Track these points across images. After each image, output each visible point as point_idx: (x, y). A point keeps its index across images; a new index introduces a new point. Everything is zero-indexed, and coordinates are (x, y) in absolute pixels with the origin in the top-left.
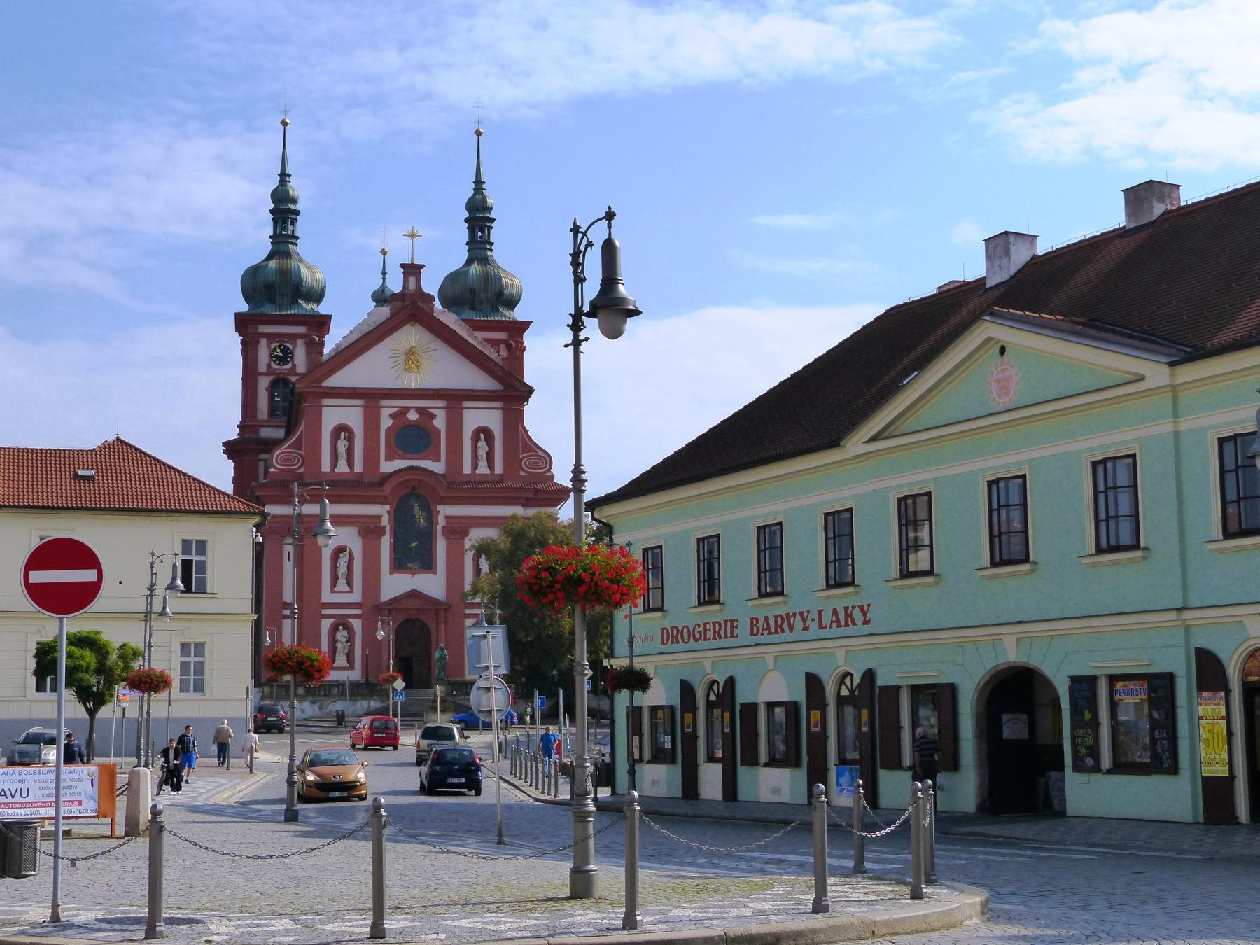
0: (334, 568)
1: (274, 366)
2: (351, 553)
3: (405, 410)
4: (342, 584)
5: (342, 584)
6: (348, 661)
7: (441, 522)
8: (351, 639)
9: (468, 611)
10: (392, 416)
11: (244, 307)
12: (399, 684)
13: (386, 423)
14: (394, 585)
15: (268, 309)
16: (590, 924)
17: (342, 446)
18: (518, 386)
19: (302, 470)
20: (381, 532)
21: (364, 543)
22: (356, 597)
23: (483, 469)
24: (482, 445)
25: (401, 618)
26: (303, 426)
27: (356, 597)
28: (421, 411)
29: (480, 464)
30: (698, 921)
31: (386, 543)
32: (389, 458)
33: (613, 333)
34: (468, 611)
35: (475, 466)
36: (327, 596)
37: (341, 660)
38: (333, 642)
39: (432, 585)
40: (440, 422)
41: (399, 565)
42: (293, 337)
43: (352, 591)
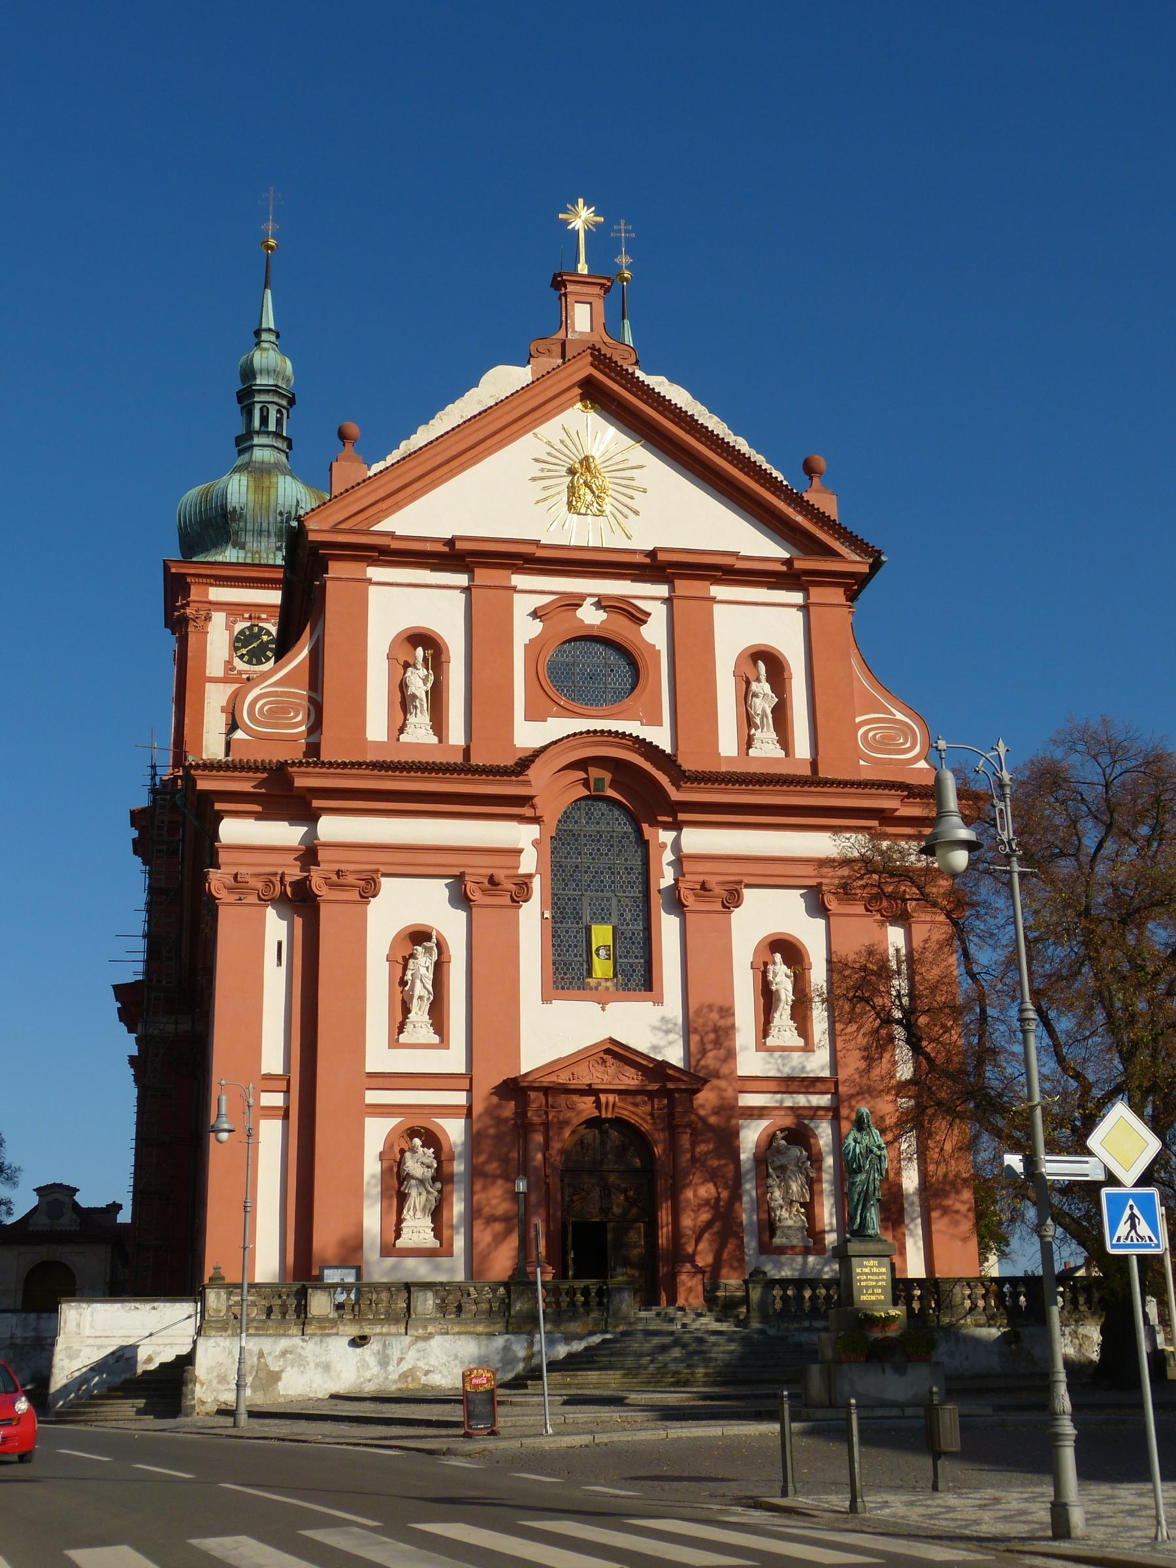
0: (401, 984)
1: (239, 665)
2: (441, 947)
3: (573, 602)
6: (437, 1232)
13: (525, 630)
14: (554, 1032)
17: (418, 682)
20: (522, 889)
23: (766, 747)
24: (763, 687)
29: (758, 734)
32: (534, 714)
35: (748, 742)
36: (379, 1056)
40: (655, 633)
41: (568, 974)
43: (444, 1043)
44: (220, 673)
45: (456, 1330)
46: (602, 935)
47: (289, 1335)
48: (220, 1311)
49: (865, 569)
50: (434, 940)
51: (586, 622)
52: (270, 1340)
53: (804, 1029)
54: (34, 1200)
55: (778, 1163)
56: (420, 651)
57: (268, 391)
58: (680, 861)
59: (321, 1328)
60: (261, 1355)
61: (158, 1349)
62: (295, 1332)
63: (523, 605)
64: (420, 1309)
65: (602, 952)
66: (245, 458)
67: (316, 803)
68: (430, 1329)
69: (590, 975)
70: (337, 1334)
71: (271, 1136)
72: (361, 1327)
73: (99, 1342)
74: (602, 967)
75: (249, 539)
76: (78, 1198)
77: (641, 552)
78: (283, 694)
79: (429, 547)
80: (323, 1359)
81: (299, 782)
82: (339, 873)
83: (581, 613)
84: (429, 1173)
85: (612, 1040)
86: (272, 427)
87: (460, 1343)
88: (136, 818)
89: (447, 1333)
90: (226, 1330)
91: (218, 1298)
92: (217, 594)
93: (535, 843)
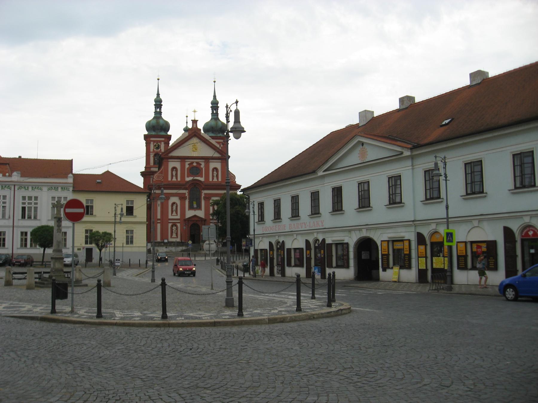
0: (172, 209)
3: (193, 163)
4: (174, 213)
5: (174, 213)
7: (203, 195)
8: (177, 229)
10: (189, 164)
11: (146, 133)
12: (190, 242)
16: (228, 315)
17: (174, 173)
22: (178, 217)
24: (215, 172)
27: (178, 217)
28: (197, 163)
30: (260, 314)
31: (187, 202)
32: (188, 177)
33: (237, 137)
35: (213, 179)
36: (170, 217)
37: (174, 235)
38: (172, 230)
39: (201, 214)
40: (203, 165)
41: (191, 207)
42: (160, 141)
58: (205, 194)
71: (159, 225)
92: (152, 139)
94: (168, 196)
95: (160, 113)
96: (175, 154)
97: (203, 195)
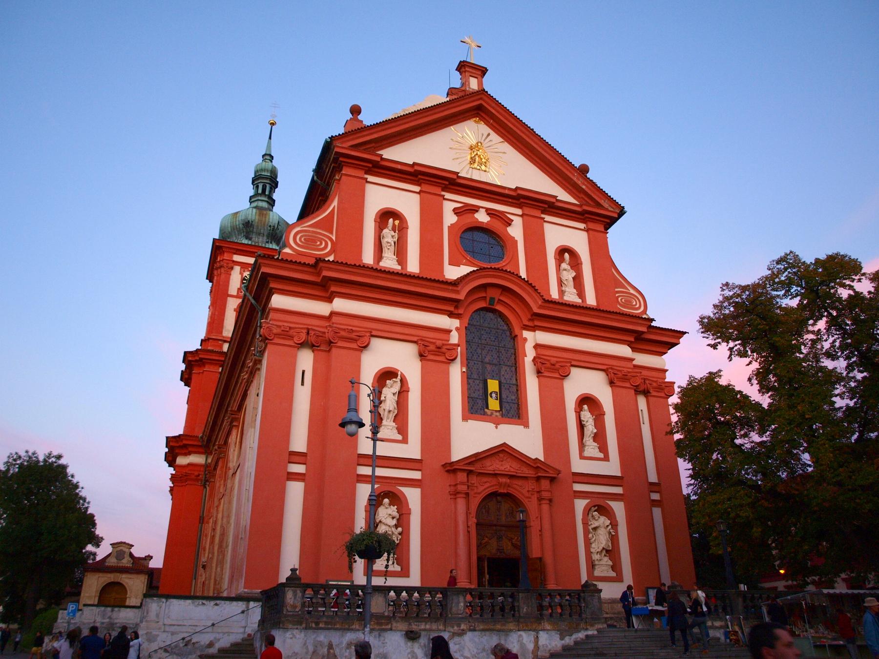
2: (403, 381)
4: (388, 429)
7: (530, 354)
9: (578, 487)
14: (470, 438)
15: (245, 241)
18: (606, 204)
19: (331, 258)
21: (423, 368)
22: (412, 450)
25: (484, 487)
26: (335, 203)
27: (412, 450)
28: (490, 212)
31: (456, 373)
34: (578, 487)
39: (528, 440)
40: (516, 231)
43: (405, 441)
44: (235, 293)
45: (482, 627)
46: (493, 385)
47: (352, 630)
48: (296, 607)
49: (616, 216)
50: (399, 377)
51: (480, 220)
52: (338, 633)
53: (603, 448)
54: (109, 550)
55: (593, 526)
56: (391, 220)
57: (267, 178)
59: (378, 624)
60: (330, 646)
61: (217, 636)
62: (357, 627)
63: (448, 208)
64: (454, 610)
65: (494, 395)
66: (254, 204)
67: (333, 289)
68: (463, 627)
69: (487, 408)
70: (391, 629)
72: (410, 624)
73: (173, 629)
74: (494, 404)
75: (254, 236)
76: (133, 550)
77: (510, 189)
78: (313, 232)
79: (399, 167)
80: (381, 650)
81: (325, 273)
82: (344, 330)
83: (477, 215)
84: (394, 522)
85: (505, 443)
86: (267, 193)
87: (485, 638)
88: (188, 357)
89: (474, 630)
90: (301, 624)
91: (295, 595)
92: (237, 258)
93: (457, 329)
94: (359, 335)
95: (272, 203)
96: (403, 153)
97: (530, 354)
